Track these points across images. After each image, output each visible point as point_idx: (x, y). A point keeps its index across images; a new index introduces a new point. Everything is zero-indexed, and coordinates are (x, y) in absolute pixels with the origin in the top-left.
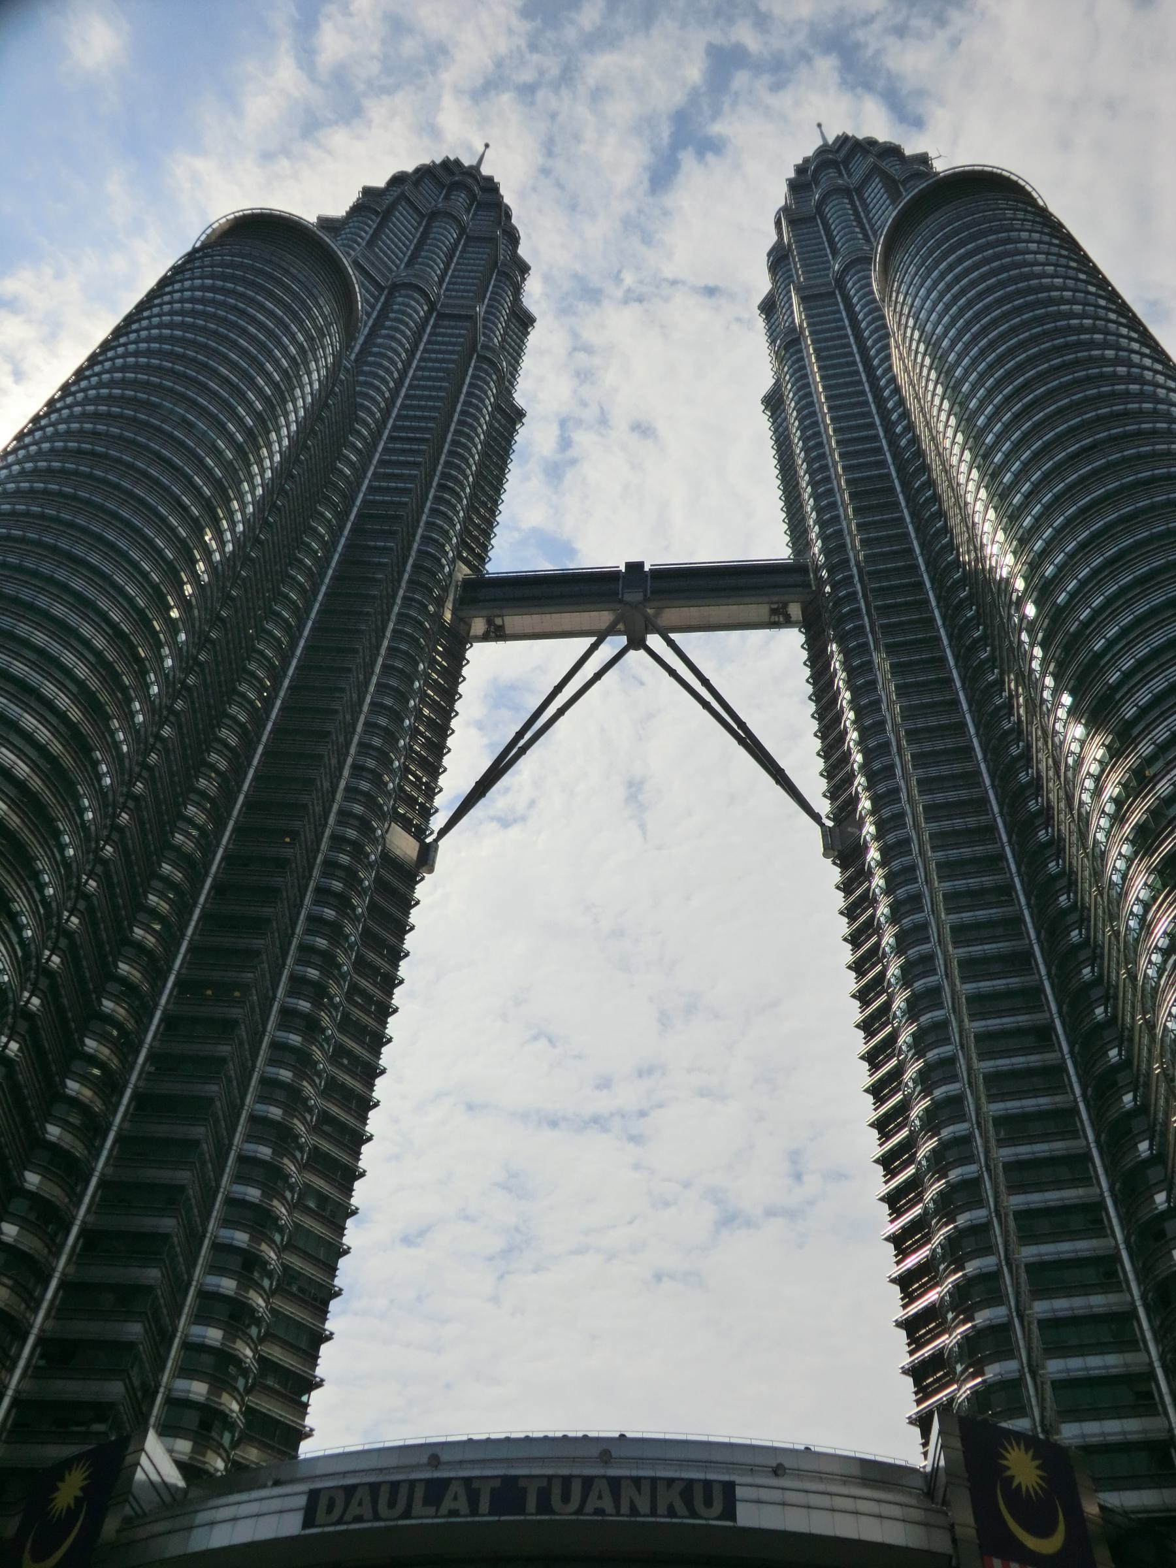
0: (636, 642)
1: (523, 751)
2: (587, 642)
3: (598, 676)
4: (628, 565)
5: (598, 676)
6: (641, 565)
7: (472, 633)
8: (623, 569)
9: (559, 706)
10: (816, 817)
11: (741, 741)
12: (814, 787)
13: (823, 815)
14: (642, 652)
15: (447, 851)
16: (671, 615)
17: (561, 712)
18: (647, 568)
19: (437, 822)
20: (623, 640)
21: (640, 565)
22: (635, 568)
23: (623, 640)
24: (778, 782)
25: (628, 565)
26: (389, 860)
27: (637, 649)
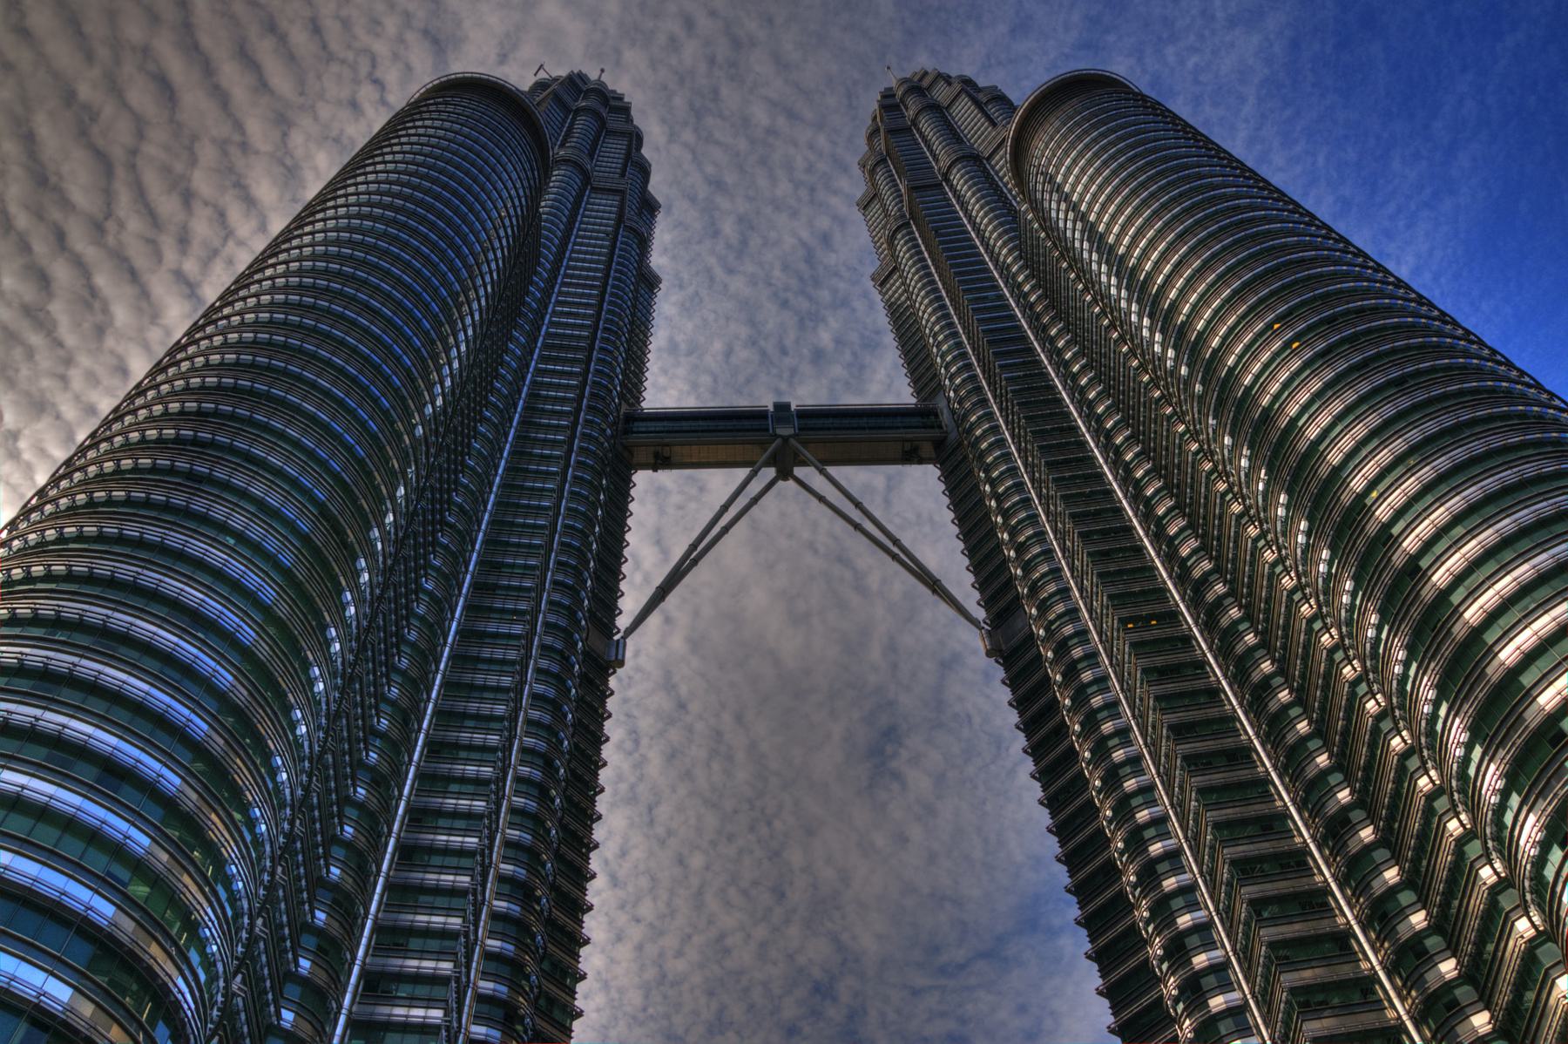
0: (785, 474)
2: (742, 473)
3: (755, 500)
6: (788, 406)
8: (771, 408)
11: (894, 557)
12: (970, 598)
13: (981, 619)
14: (791, 483)
18: (793, 407)
24: (934, 591)
27: (785, 479)
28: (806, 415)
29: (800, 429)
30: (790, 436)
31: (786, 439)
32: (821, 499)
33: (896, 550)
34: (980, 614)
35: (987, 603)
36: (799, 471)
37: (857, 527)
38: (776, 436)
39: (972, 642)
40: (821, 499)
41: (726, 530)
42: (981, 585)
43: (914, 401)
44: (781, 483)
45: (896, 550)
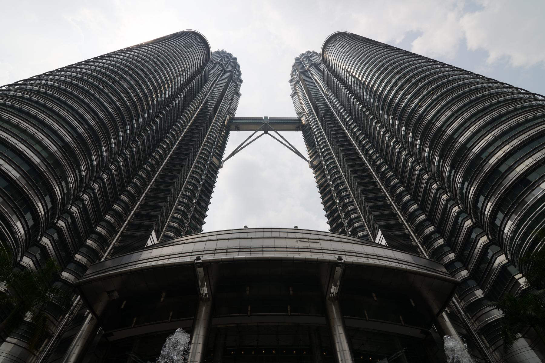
0: (266, 133)
1: (242, 148)
3: (258, 137)
4: (265, 117)
5: (258, 137)
6: (267, 117)
7: (231, 129)
8: (263, 118)
10: (307, 161)
11: (290, 148)
12: (307, 156)
14: (268, 135)
15: (225, 164)
17: (250, 142)
18: (269, 118)
19: (223, 159)
20: (263, 132)
21: (267, 117)
23: (263, 132)
25: (265, 117)
26: (212, 163)
27: (266, 134)
28: (271, 120)
30: (268, 123)
31: (266, 124)
32: (274, 137)
33: (290, 147)
34: (309, 159)
36: (269, 132)
37: (282, 142)
38: (264, 123)
39: (307, 165)
40: (274, 137)
41: (250, 142)
43: (297, 117)
44: (264, 134)
45: (290, 147)
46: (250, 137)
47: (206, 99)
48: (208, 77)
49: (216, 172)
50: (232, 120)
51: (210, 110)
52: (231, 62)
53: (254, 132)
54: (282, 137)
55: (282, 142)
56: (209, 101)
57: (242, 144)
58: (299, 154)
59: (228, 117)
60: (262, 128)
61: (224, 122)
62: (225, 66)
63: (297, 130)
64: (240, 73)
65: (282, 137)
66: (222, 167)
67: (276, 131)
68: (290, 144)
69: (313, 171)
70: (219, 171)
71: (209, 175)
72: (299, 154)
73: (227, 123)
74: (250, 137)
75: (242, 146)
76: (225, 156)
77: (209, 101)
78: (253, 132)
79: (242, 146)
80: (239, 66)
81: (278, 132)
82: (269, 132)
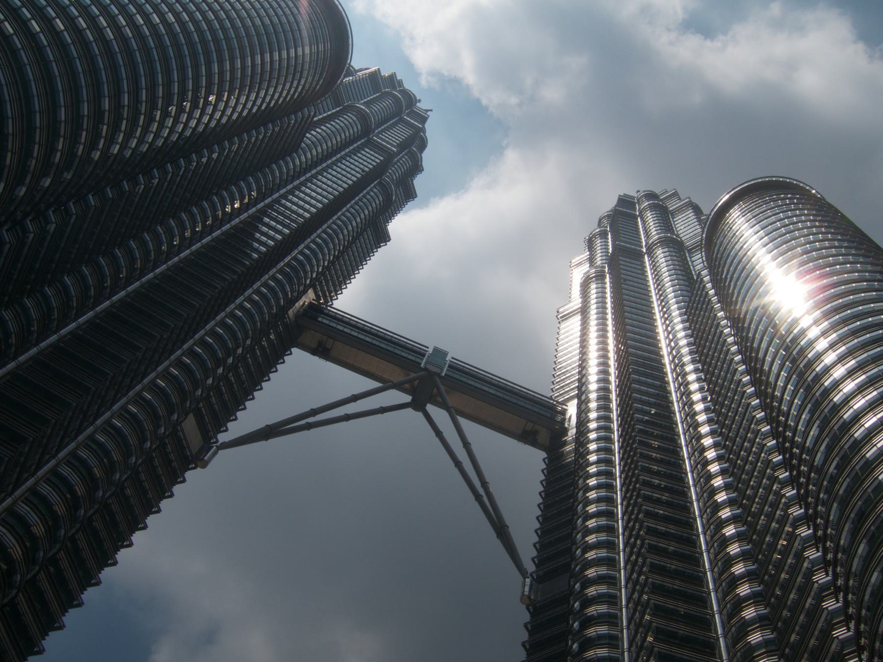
0: (418, 405)
1: (309, 426)
4: (436, 350)
8: (430, 350)
9: (349, 413)
11: (478, 497)
14: (420, 415)
16: (453, 400)
17: (347, 418)
18: (448, 358)
19: (222, 438)
20: (408, 398)
21: (445, 354)
22: (439, 353)
29: (446, 374)
30: (439, 375)
32: (439, 434)
33: (481, 491)
34: (531, 567)
35: (540, 562)
36: (430, 408)
37: (458, 464)
38: (426, 369)
40: (439, 434)
41: (347, 418)
42: (542, 546)
44: (410, 410)
45: (481, 491)
46: (355, 398)
47: (259, 206)
48: (302, 141)
49: (176, 477)
50: (316, 311)
51: (256, 251)
52: (402, 120)
53: (376, 385)
54: (466, 445)
55: (458, 464)
56: (266, 220)
57: (314, 412)
58: (501, 530)
59: (310, 296)
60: (410, 381)
61: (284, 310)
62: (378, 126)
63: (528, 437)
64: (416, 168)
65: (466, 445)
66: (204, 465)
67: (454, 413)
68: (484, 484)
69: (527, 617)
70: (189, 475)
71: (128, 492)
72: (501, 530)
73: (297, 316)
74: (355, 398)
75: (311, 420)
76: (236, 428)
77: (266, 220)
78: (375, 384)
79: (311, 420)
80: (423, 145)
81: (462, 420)
82: (430, 408)
